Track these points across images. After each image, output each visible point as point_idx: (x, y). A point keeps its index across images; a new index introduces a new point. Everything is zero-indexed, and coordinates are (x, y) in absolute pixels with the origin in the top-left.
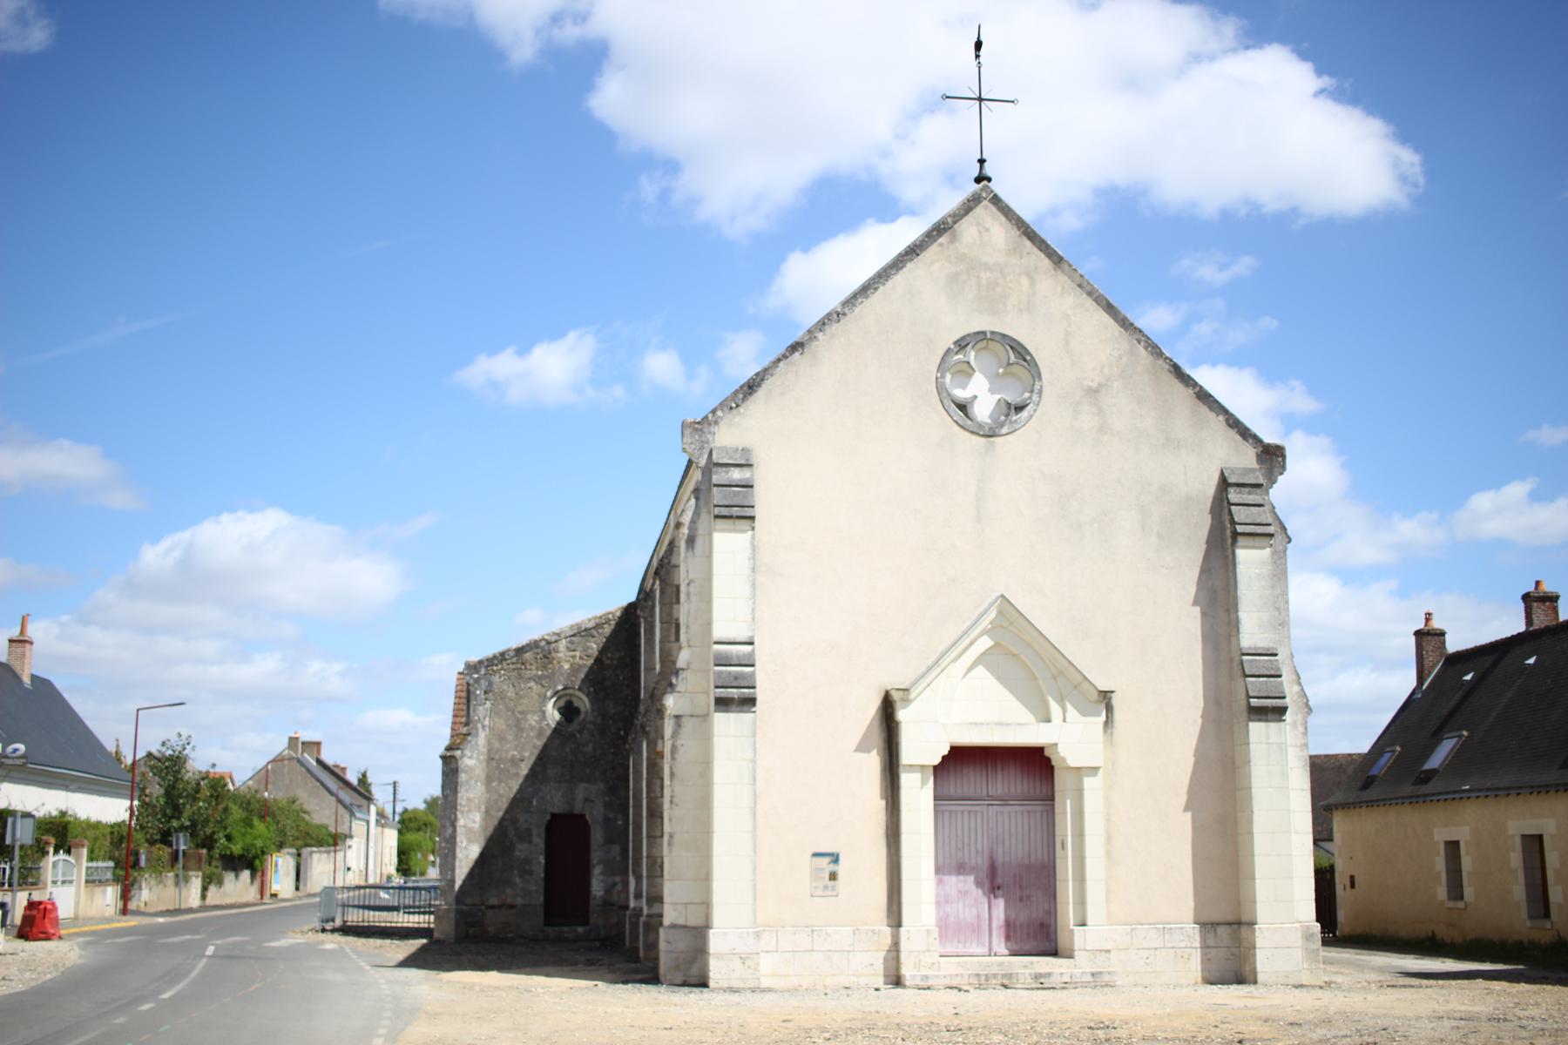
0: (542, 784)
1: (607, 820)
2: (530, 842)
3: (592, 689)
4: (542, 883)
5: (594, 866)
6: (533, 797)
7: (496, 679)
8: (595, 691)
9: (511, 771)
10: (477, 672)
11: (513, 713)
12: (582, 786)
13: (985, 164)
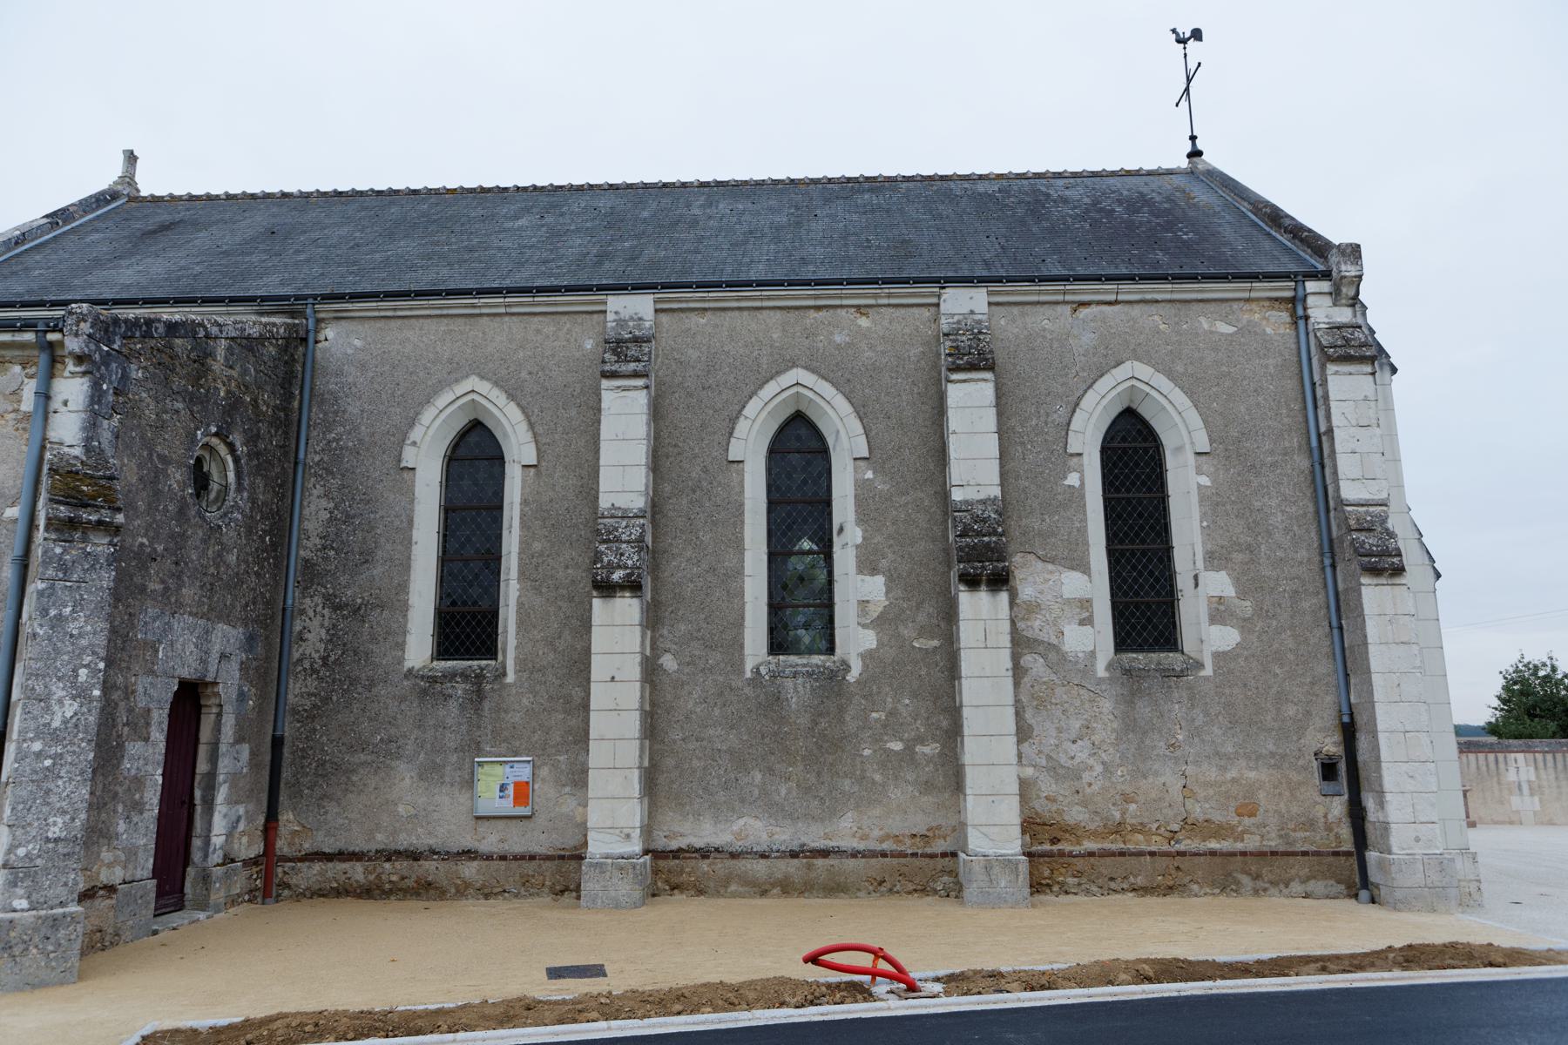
0: (173, 615)
1: (242, 696)
2: (146, 740)
3: (245, 448)
4: (153, 827)
5: (220, 785)
6: (160, 643)
7: (136, 374)
8: (249, 455)
9: (135, 579)
10: (109, 343)
11: (150, 455)
12: (222, 627)
13: (1197, 141)
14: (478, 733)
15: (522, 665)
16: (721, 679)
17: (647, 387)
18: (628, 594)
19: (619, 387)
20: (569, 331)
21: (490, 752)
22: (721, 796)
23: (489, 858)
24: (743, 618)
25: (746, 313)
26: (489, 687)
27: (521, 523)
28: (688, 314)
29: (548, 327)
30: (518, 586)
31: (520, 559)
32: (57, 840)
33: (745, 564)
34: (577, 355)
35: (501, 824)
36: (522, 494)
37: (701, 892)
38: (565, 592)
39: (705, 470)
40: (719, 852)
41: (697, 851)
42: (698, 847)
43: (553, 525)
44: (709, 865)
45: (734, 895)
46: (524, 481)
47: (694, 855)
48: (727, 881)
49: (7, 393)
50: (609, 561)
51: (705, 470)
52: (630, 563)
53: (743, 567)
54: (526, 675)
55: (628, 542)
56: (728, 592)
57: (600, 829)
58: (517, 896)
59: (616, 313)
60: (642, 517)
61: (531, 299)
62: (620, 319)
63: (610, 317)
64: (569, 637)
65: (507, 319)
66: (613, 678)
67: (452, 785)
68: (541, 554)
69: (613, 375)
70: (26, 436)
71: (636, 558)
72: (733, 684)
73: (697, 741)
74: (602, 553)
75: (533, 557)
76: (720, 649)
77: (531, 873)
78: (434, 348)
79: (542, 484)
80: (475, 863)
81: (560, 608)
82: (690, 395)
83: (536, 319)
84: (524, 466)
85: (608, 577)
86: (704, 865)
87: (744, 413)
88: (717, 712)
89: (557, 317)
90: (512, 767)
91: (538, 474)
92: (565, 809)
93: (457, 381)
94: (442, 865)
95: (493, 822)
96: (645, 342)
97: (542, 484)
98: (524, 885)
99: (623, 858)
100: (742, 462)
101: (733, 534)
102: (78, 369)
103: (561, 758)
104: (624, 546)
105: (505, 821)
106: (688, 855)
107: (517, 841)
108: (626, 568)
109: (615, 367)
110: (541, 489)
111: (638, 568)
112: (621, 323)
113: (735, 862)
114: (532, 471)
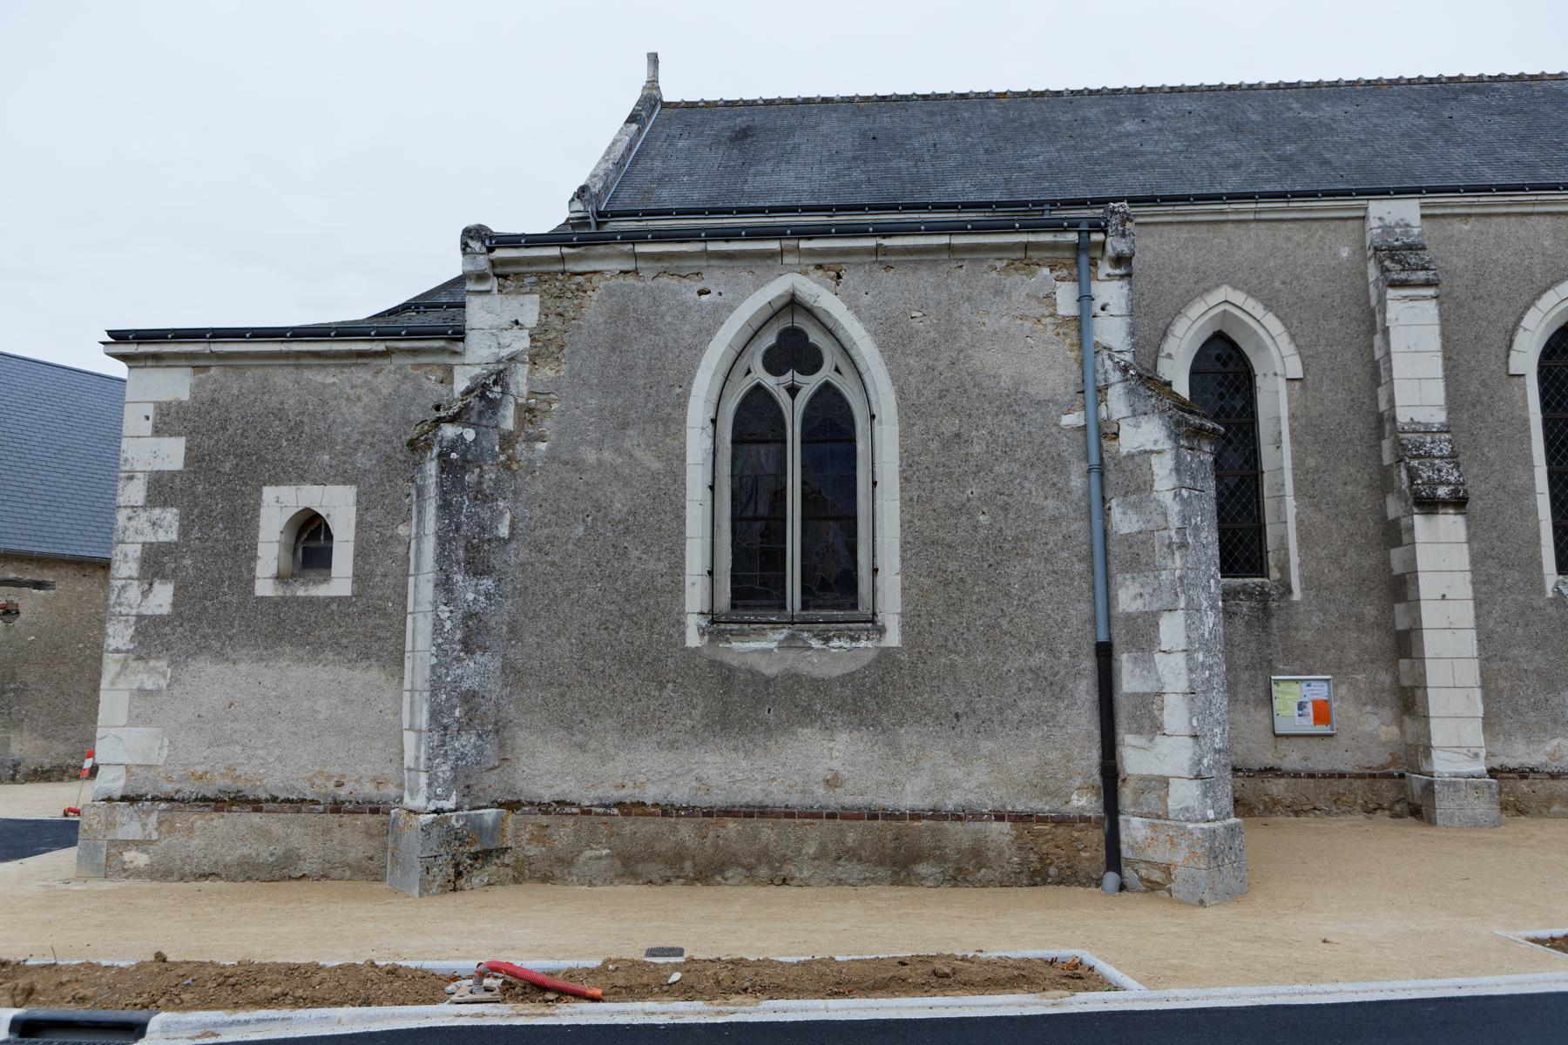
14: (1268, 652)
15: (1307, 583)
16: (1521, 598)
17: (1436, 297)
18: (1451, 511)
19: (1406, 297)
20: (1322, 239)
21: (1283, 670)
22: (1532, 717)
23: (1297, 775)
24: (1538, 536)
25: (1513, 219)
26: (1275, 604)
27: (1291, 438)
28: (1449, 220)
29: (1299, 233)
30: (1294, 503)
31: (1295, 475)
32: (1219, 751)
33: (1537, 481)
34: (1334, 263)
35: (1302, 742)
36: (1289, 409)
37: (1521, 812)
38: (1345, 509)
39: (1484, 384)
40: (1535, 772)
41: (1511, 771)
42: (1511, 767)
43: (1325, 440)
44: (1529, 786)
45: (1557, 816)
46: (1289, 395)
47: (1511, 775)
48: (1549, 801)
49: (1041, 296)
50: (1429, 477)
51: (1484, 384)
52: (1452, 479)
53: (1534, 484)
54: (1313, 593)
55: (1442, 458)
56: (1520, 509)
57: (1443, 748)
58: (1329, 813)
59: (1380, 219)
60: (1446, 432)
61: (1286, 205)
62: (1385, 226)
63: (1374, 223)
64: (1354, 555)
65: (1253, 225)
66: (1444, 596)
67: (1246, 703)
68: (1316, 470)
69: (1404, 284)
70: (1068, 341)
71: (1456, 474)
72: (1535, 604)
73: (1501, 660)
74: (1417, 469)
75: (1308, 473)
76: (1517, 568)
77: (1341, 791)
78: (1177, 256)
79: (1309, 398)
80: (1282, 781)
81: (1343, 525)
82: (1460, 305)
83: (1285, 226)
84: (1288, 380)
85: (1435, 495)
86: (1523, 786)
87: (1522, 324)
88: (1520, 631)
89: (1309, 224)
90: (1309, 685)
91: (1304, 387)
92: (1367, 728)
93: (1208, 290)
94: (1247, 782)
95: (1293, 739)
96: (1420, 249)
97: (1309, 398)
98: (1335, 802)
99: (1473, 777)
100: (1523, 375)
101: (1520, 451)
102: (1118, 272)
103: (1359, 677)
104: (1437, 461)
105: (1306, 739)
106: (1505, 775)
107: (1322, 759)
108: (1449, 484)
109: (1403, 276)
110: (1308, 404)
111: (1463, 484)
112: (1387, 229)
113: (1555, 782)
114: (1298, 384)
